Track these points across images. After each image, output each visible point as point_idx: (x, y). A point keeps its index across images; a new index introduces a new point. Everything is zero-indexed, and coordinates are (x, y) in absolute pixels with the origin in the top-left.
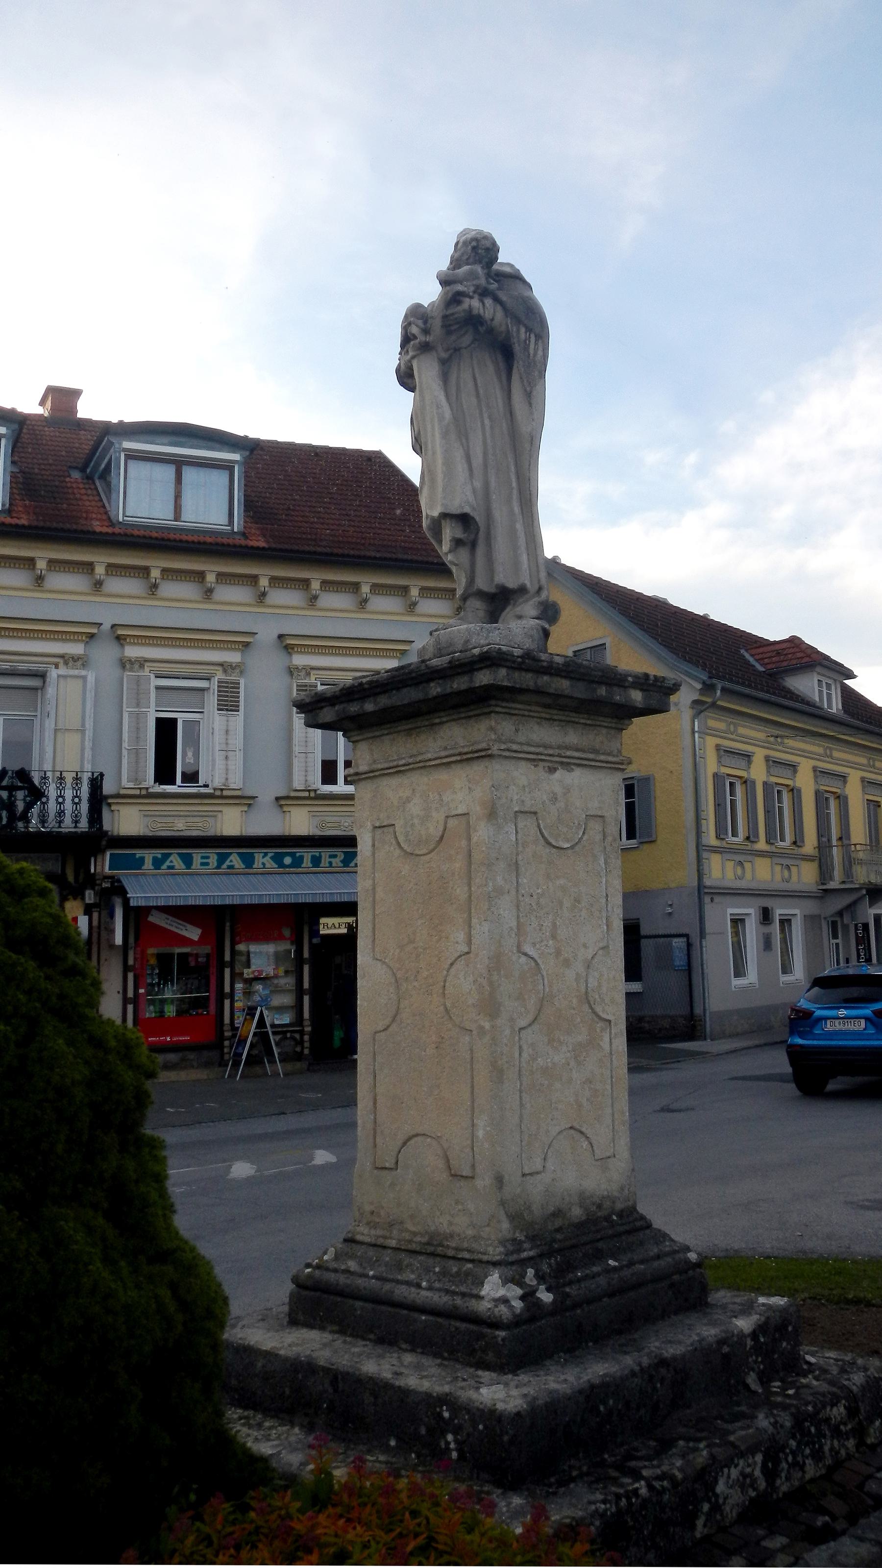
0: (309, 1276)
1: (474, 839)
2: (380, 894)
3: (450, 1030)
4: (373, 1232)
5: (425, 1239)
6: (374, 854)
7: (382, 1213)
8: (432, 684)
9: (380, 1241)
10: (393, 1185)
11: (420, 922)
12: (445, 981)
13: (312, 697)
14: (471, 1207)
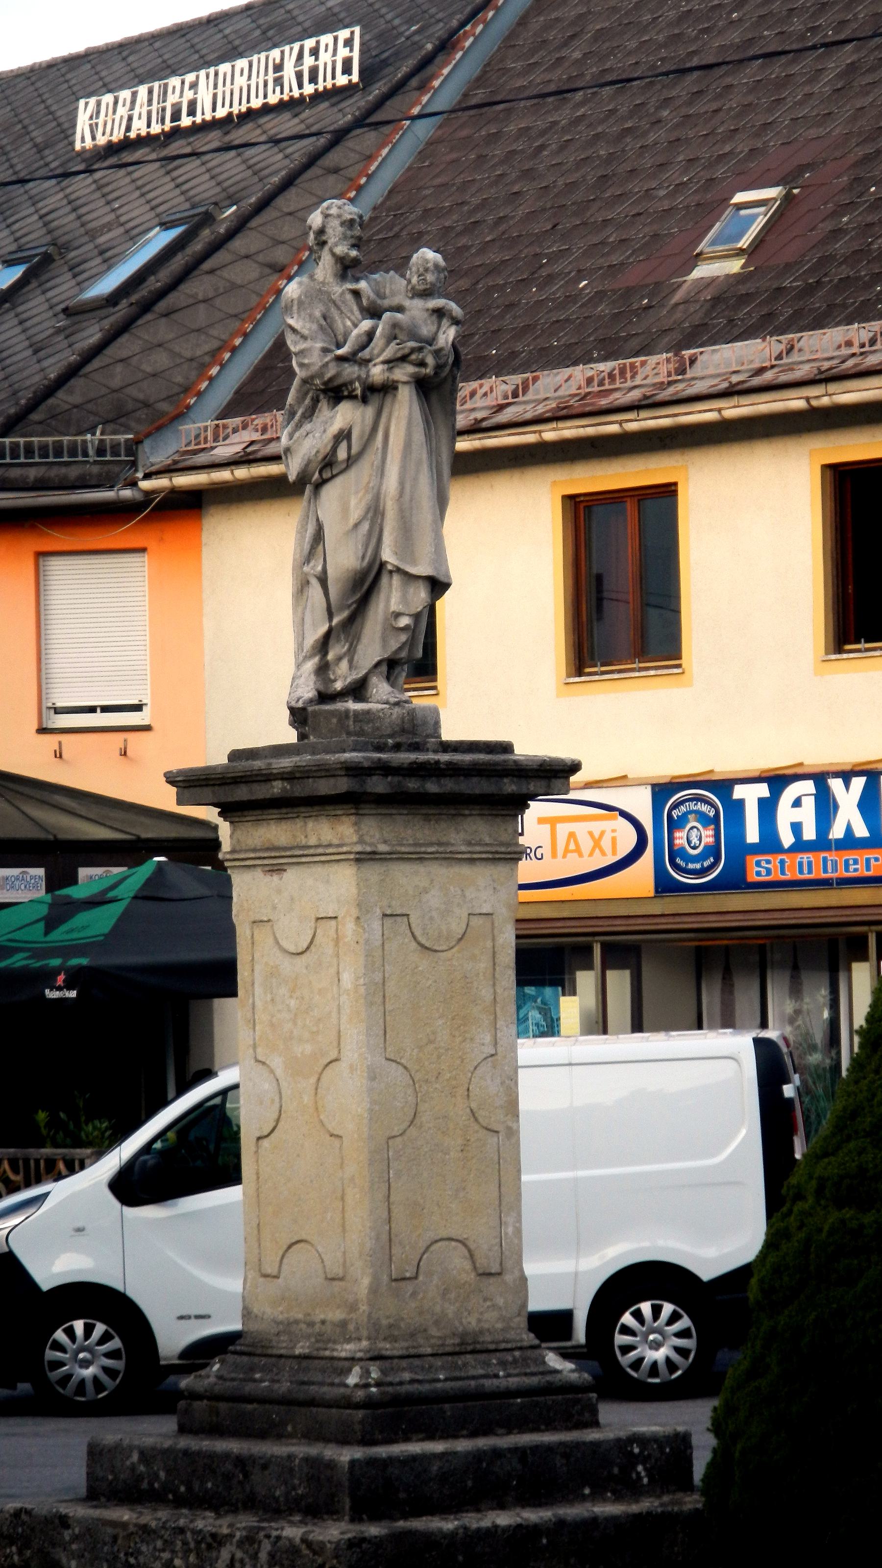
3: (477, 1132)
4: (397, 1345)
7: (402, 1325)
8: (505, 780)
9: (412, 1351)
10: (414, 1294)
11: (440, 1022)
13: (373, 762)
14: (500, 1301)
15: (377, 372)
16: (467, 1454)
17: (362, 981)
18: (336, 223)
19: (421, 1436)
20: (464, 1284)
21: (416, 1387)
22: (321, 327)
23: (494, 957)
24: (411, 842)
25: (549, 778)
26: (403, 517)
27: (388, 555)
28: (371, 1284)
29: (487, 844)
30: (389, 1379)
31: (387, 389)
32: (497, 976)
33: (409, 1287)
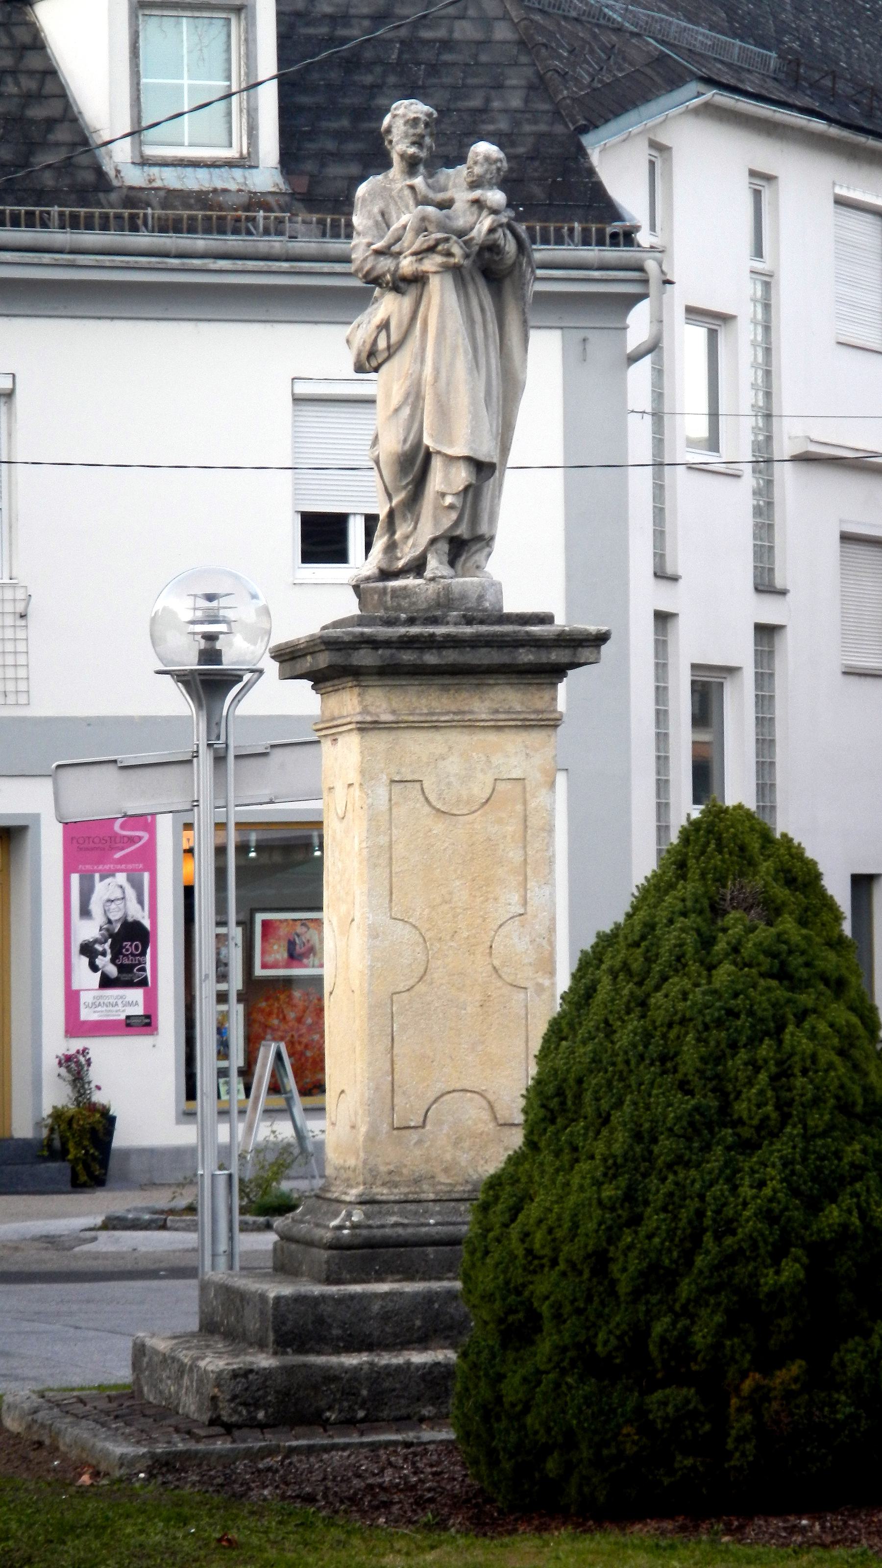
0: (352, 1235)
1: (532, 804)
2: (399, 849)
3: (500, 988)
4: (396, 1191)
5: (469, 1187)
6: (390, 809)
7: (405, 1171)
8: (521, 650)
9: (411, 1197)
10: (420, 1142)
12: (492, 941)
15: (407, 265)
16: (416, 1294)
17: (364, 845)
18: (400, 122)
19: (398, 1277)
20: (481, 1134)
21: (400, 1230)
22: (377, 223)
23: (525, 821)
24: (425, 711)
25: (575, 647)
26: (439, 401)
27: (427, 441)
28: (367, 1133)
29: (519, 712)
30: (371, 1222)
31: (419, 280)
32: (528, 838)
33: (414, 1136)
